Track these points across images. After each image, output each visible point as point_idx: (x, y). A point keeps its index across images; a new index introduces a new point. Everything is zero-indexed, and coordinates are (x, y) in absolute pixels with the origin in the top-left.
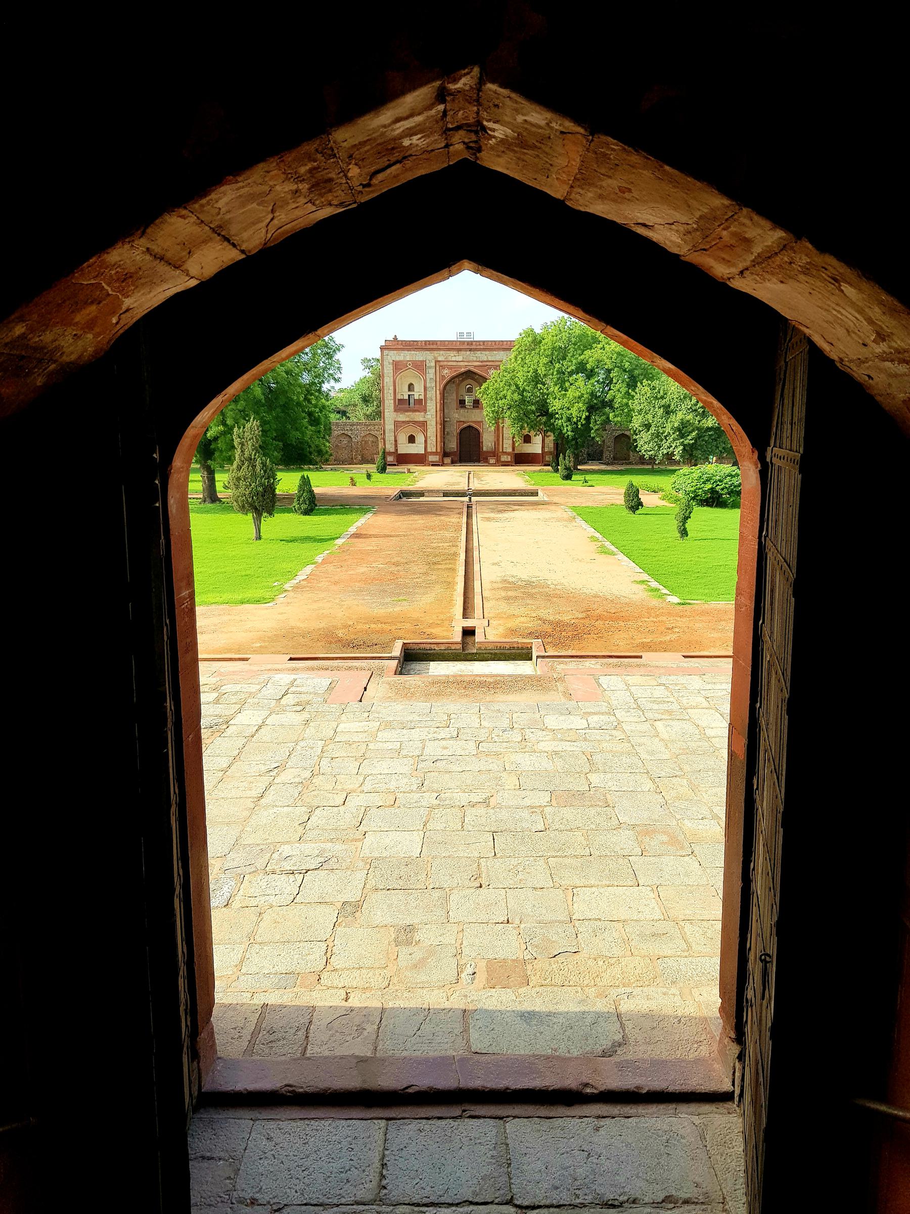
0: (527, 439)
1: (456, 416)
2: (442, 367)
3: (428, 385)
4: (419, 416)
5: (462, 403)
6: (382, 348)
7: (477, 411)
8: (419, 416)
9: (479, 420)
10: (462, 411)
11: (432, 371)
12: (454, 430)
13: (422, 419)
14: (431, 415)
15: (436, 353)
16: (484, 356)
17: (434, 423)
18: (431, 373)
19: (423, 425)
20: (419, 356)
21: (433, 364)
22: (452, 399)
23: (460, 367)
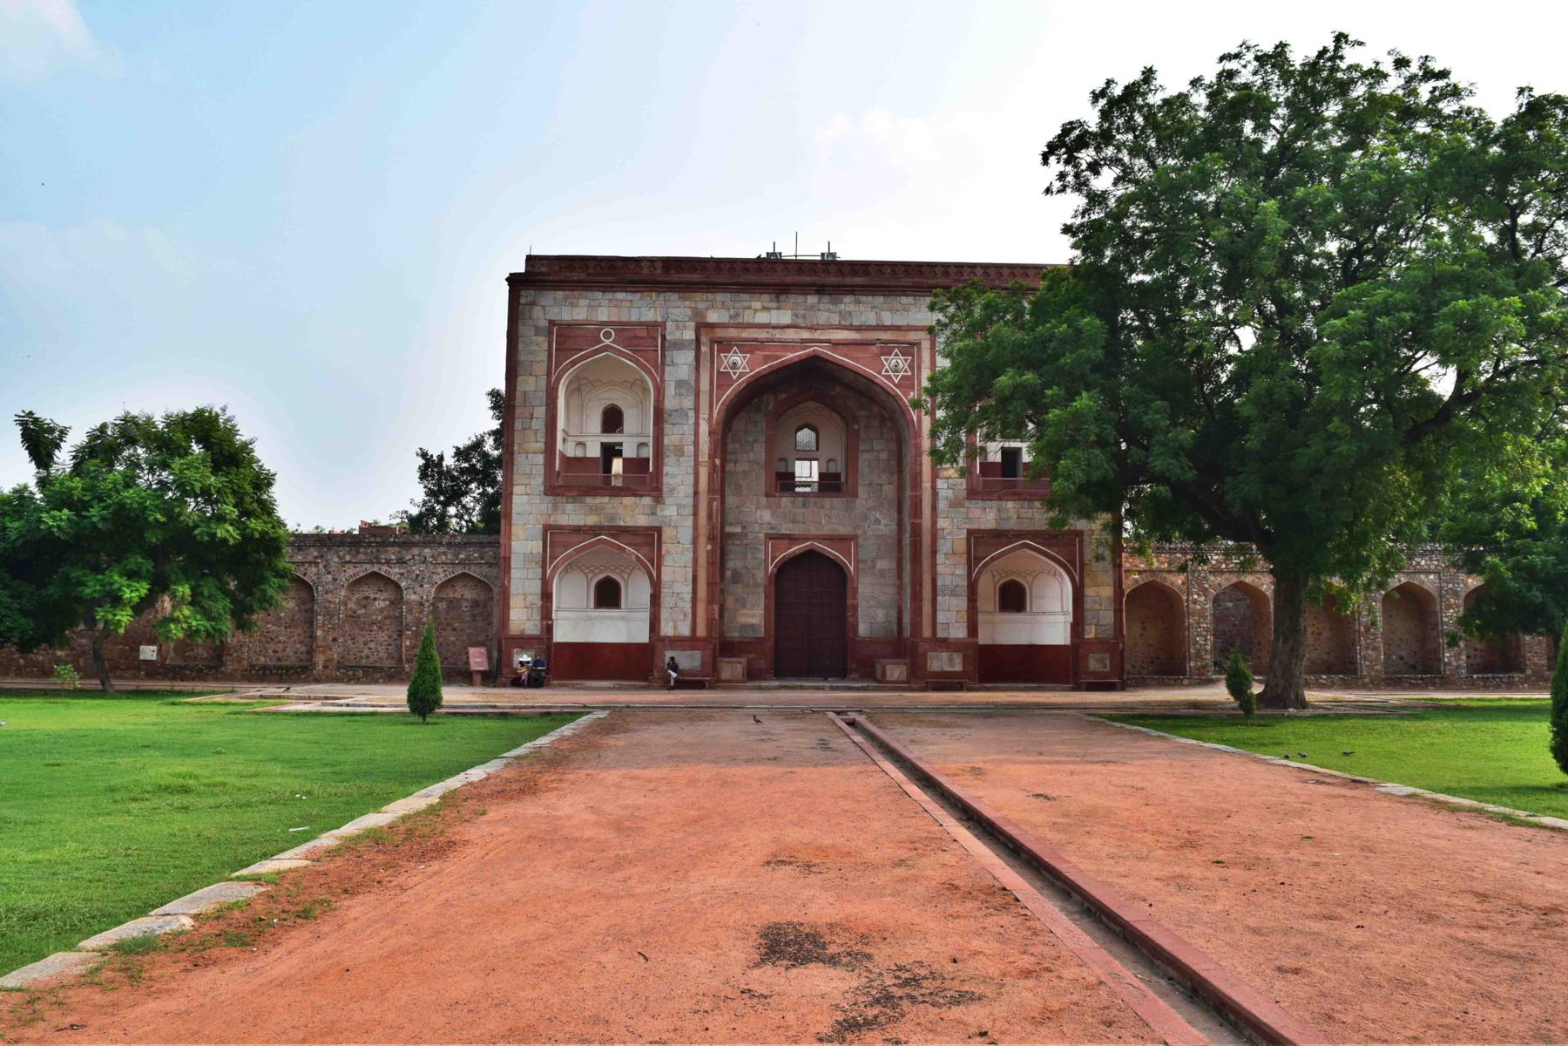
0: (1013, 598)
1: (766, 516)
2: (725, 345)
3: (670, 403)
4: (634, 512)
5: (785, 482)
6: (516, 282)
7: (834, 503)
8: (634, 512)
9: (843, 530)
10: (786, 501)
11: (685, 358)
12: (758, 564)
13: (642, 521)
14: (677, 511)
15: (700, 300)
16: (868, 311)
17: (686, 535)
18: (681, 364)
19: (650, 539)
20: (641, 308)
21: (690, 335)
22: (752, 459)
23: (786, 345)
